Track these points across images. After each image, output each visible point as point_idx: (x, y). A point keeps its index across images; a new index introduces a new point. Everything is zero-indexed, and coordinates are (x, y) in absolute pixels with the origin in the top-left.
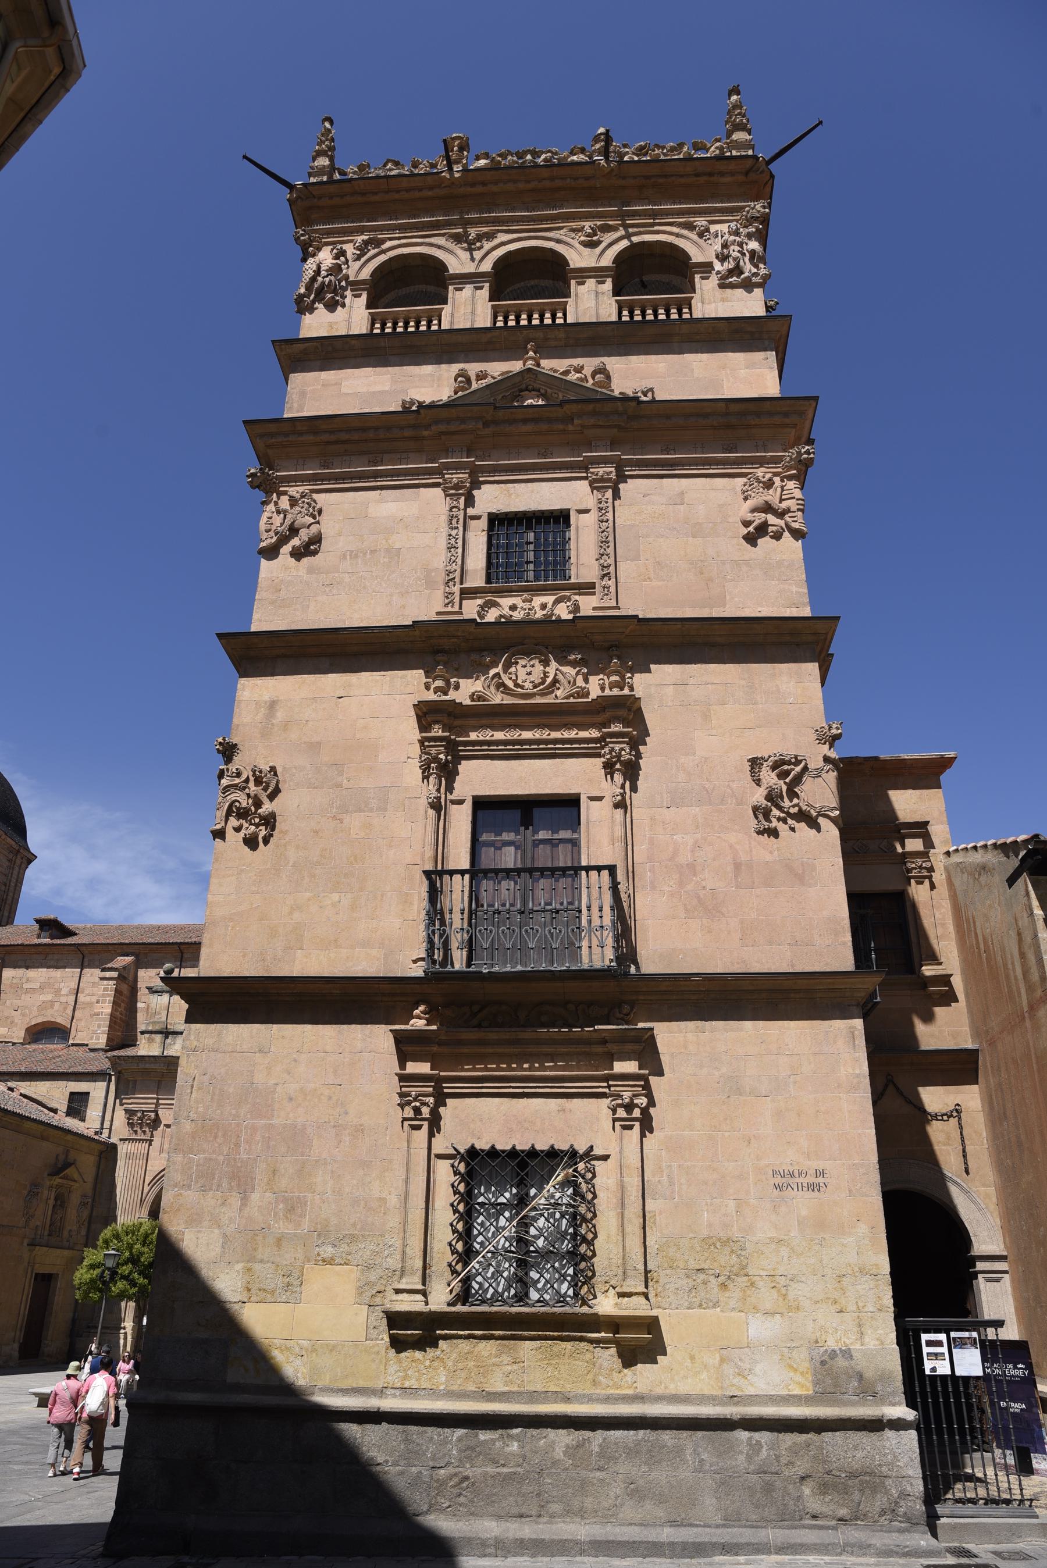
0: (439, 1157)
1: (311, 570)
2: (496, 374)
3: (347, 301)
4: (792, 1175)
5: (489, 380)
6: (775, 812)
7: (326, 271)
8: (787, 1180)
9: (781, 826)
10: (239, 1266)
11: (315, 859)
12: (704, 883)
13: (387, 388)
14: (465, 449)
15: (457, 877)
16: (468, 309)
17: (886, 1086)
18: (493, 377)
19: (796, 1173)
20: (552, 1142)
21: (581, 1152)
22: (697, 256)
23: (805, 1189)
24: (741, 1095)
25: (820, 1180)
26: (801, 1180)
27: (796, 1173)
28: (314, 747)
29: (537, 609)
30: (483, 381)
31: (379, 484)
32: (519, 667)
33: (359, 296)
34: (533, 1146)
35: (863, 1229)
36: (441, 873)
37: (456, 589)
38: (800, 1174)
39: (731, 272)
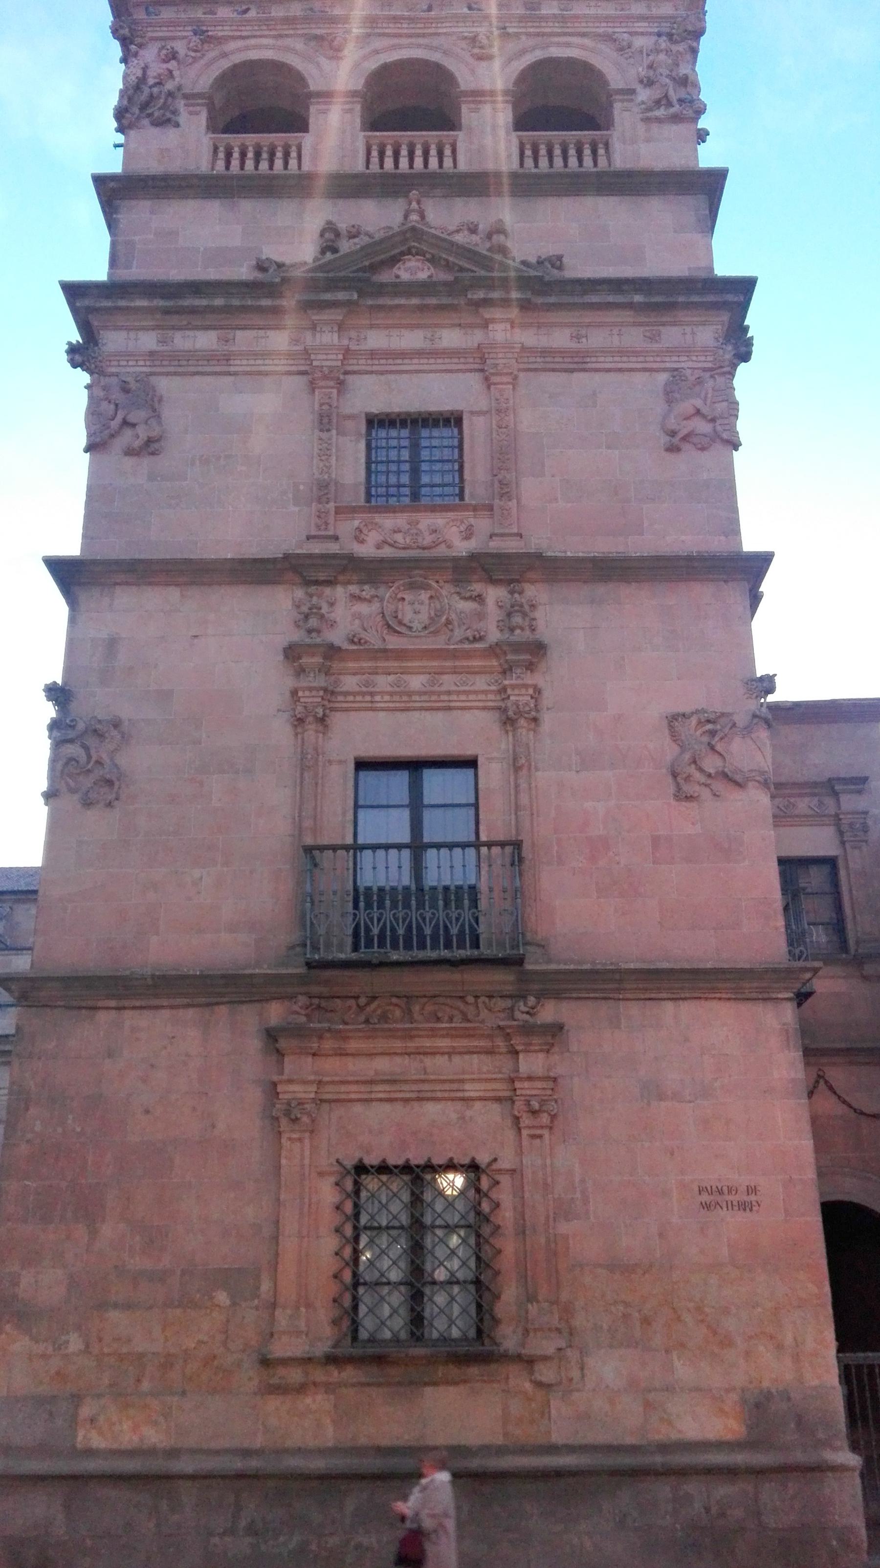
0: (321, 1174)
1: (151, 477)
2: (370, 229)
3: (183, 118)
5: (364, 240)
6: (697, 775)
7: (155, 78)
9: (705, 793)
11: (171, 829)
12: (617, 858)
13: (237, 242)
14: (336, 329)
15: (341, 853)
16: (334, 138)
17: (817, 1082)
18: (367, 234)
19: (725, 1189)
20: (450, 1155)
21: (483, 1166)
22: (615, 79)
23: (736, 1208)
24: (661, 1100)
25: (753, 1198)
26: (730, 1198)
27: (725, 1189)
28: (164, 696)
29: (426, 534)
30: (356, 240)
31: (232, 369)
32: (406, 602)
33: (197, 113)
34: (429, 1160)
36: (322, 848)
37: (331, 506)
38: (730, 1191)
39: (658, 103)
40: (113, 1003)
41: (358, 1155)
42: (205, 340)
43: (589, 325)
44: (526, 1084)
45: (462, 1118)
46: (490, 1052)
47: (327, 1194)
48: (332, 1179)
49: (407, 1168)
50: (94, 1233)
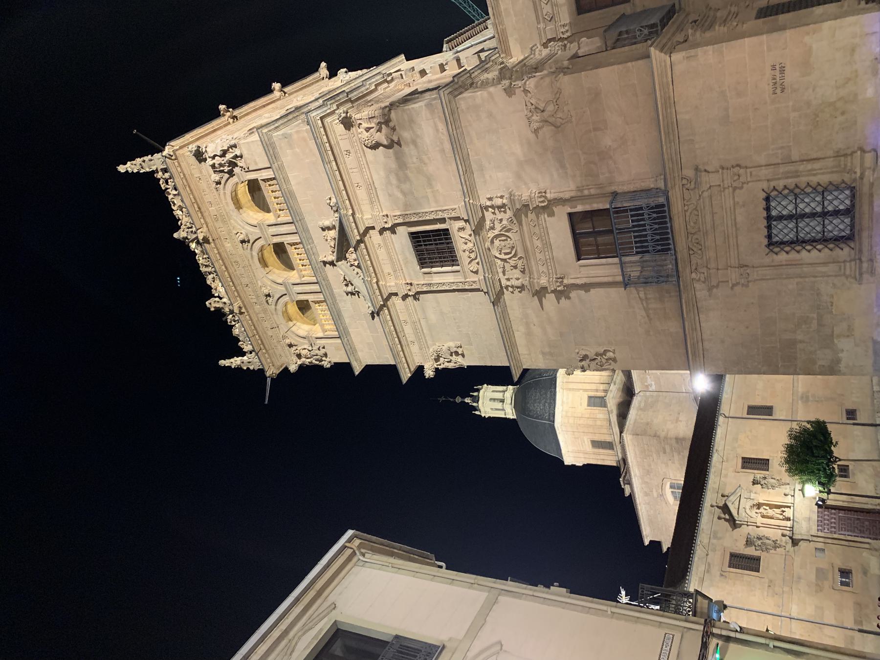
4: (775, 83)
8: (778, 85)
10: (836, 341)
25: (777, 67)
35: (807, 39)
38: (774, 79)
40: (700, 344)
41: (763, 246)
42: (408, 330)
43: (351, 183)
44: (726, 182)
45: (744, 206)
46: (711, 197)
47: (783, 257)
48: (775, 256)
49: (769, 227)
50: (801, 342)
